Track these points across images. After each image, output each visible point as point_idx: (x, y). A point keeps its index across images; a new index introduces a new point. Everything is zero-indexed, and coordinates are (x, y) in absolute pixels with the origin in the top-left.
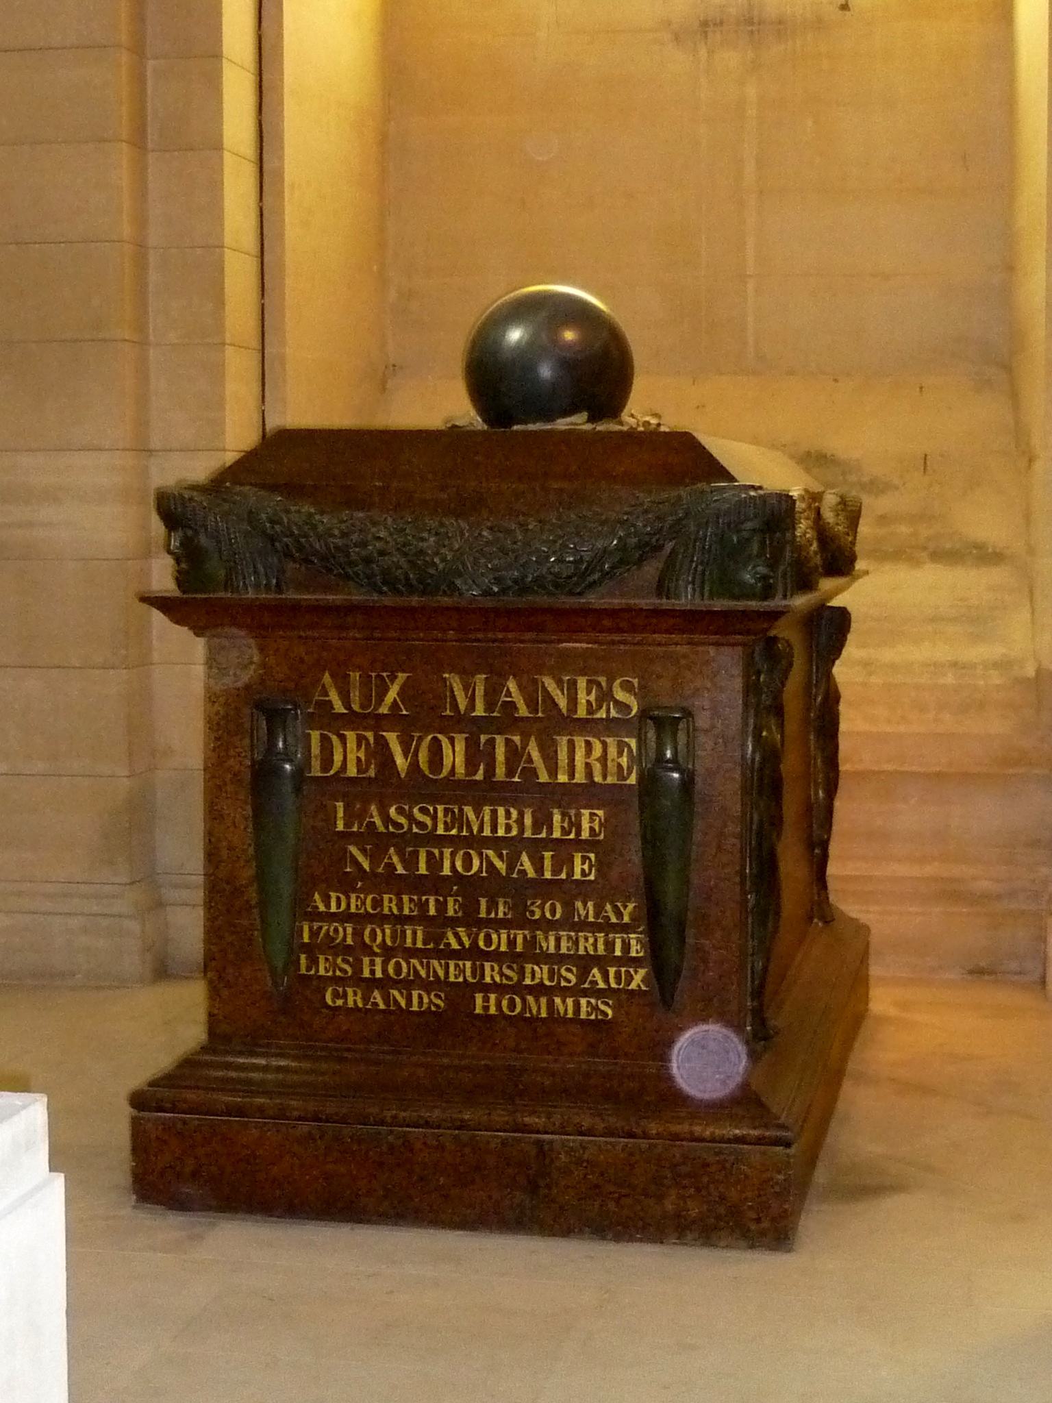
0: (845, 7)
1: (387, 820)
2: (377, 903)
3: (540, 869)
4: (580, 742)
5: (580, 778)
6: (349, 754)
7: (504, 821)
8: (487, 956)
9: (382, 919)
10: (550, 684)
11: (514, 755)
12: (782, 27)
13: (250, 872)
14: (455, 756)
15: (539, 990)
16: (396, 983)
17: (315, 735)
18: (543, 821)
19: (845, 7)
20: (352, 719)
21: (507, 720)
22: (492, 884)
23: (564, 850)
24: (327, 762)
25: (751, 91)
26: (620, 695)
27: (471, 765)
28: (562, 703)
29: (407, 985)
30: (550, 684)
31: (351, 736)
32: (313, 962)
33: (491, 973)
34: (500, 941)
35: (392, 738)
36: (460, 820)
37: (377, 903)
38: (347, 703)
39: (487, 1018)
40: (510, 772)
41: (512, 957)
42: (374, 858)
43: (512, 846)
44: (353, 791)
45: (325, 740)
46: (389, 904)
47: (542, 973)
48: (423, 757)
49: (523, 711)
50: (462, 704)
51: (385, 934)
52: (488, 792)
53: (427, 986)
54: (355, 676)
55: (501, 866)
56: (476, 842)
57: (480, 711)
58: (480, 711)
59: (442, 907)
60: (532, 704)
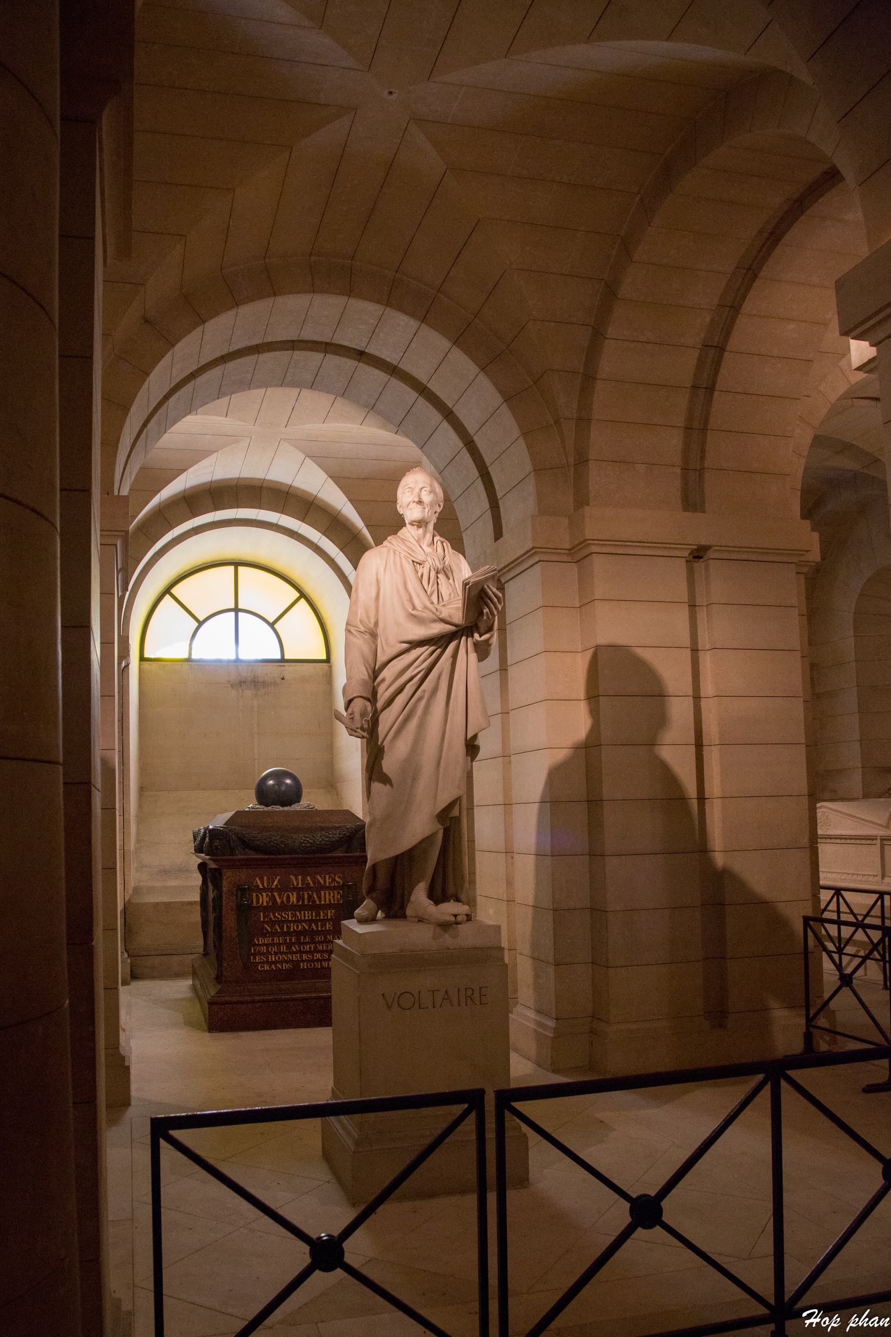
0: (283, 679)
1: (275, 917)
2: (273, 940)
3: (317, 927)
4: (327, 892)
5: (327, 902)
6: (264, 899)
7: (307, 915)
8: (304, 952)
9: (273, 944)
10: (319, 878)
11: (310, 897)
12: (264, 684)
13: (235, 934)
14: (293, 898)
15: (318, 960)
16: (278, 962)
17: (254, 895)
18: (318, 914)
19: (283, 679)
20: (265, 890)
21: (307, 887)
22: (304, 932)
23: (324, 922)
24: (258, 902)
25: (255, 703)
26: (337, 879)
27: (298, 901)
28: (322, 882)
29: (281, 962)
30: (319, 878)
31: (264, 894)
32: (255, 958)
33: (304, 957)
34: (307, 948)
35: (276, 894)
36: (294, 915)
37: (273, 940)
38: (263, 885)
39: (304, 969)
40: (309, 902)
41: (310, 952)
42: (272, 928)
43: (310, 922)
44: (266, 909)
45: (257, 895)
46: (276, 940)
47: (319, 956)
48: (285, 899)
49: (312, 885)
50: (295, 883)
51: (275, 949)
52: (303, 908)
53: (287, 962)
54: (265, 878)
55: (307, 927)
56: (300, 921)
57: (300, 885)
58: (300, 885)
59: (291, 940)
60: (314, 883)
